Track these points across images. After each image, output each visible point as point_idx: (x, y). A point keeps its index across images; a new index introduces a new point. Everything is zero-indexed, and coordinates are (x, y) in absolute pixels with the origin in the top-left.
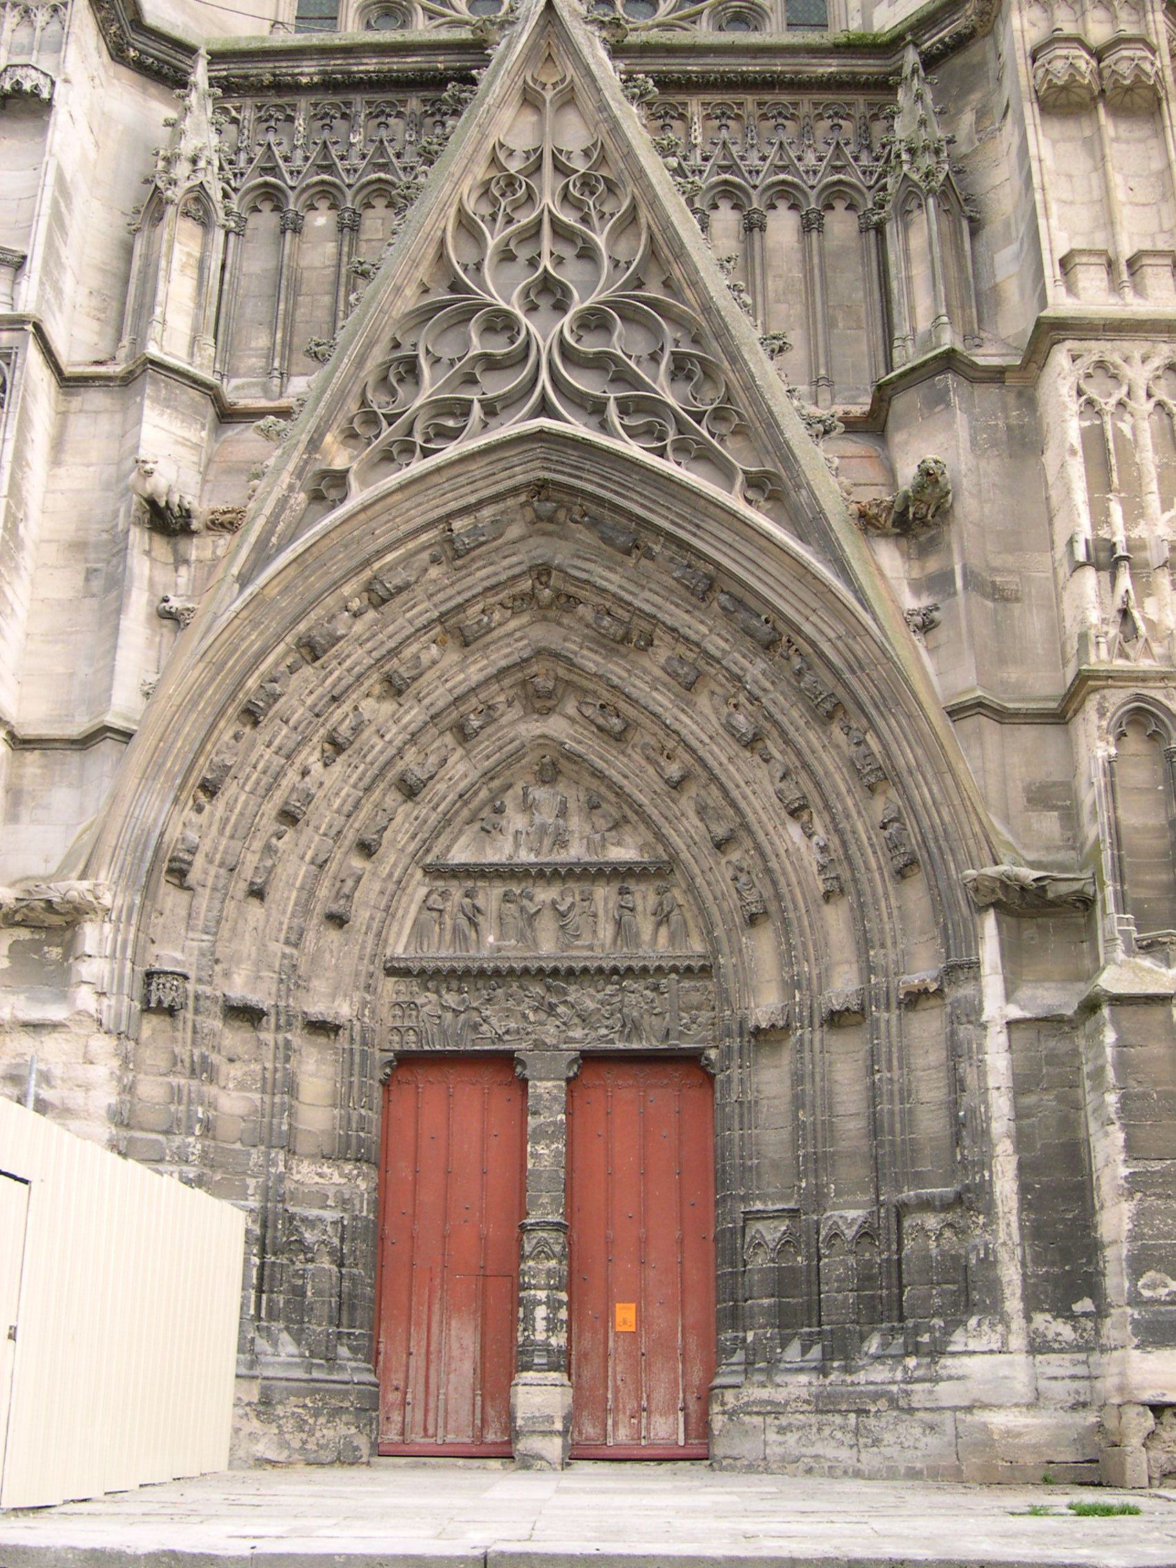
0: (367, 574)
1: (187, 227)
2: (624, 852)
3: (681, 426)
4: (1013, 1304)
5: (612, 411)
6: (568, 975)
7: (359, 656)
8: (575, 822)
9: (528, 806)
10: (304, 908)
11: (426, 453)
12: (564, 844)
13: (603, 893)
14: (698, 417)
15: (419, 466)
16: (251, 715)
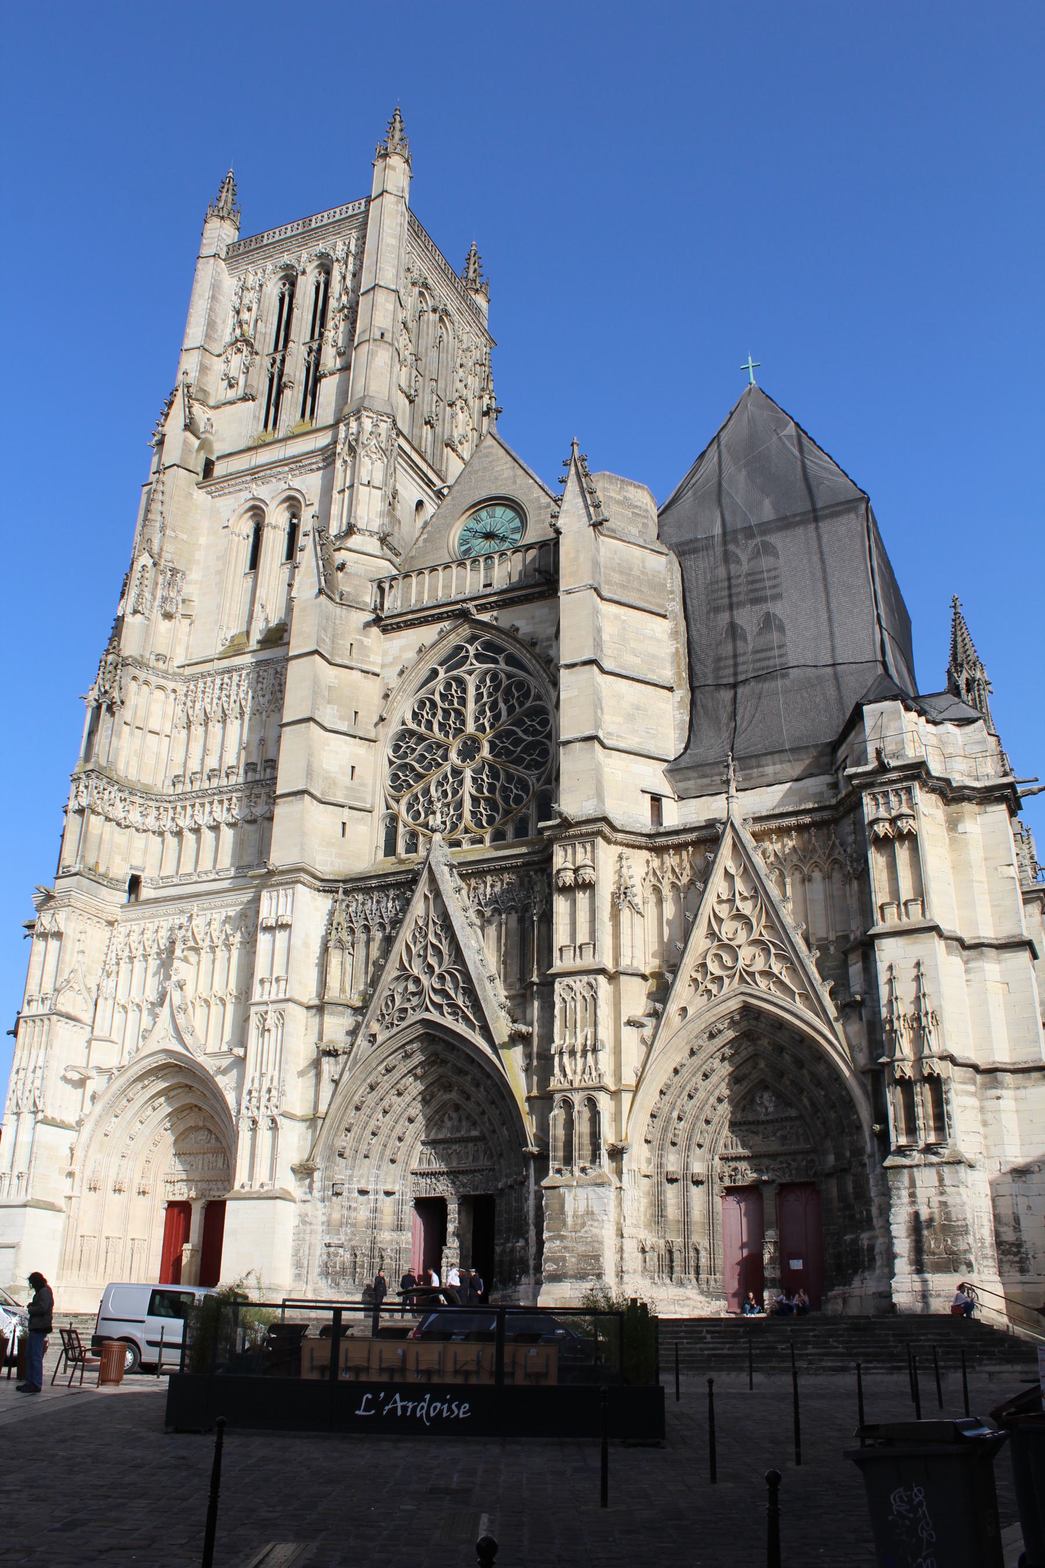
0: (385, 1063)
1: (338, 952)
2: (475, 1133)
3: (463, 1012)
4: (531, 1271)
5: (445, 1008)
6: (459, 1172)
7: (387, 1086)
8: (464, 1123)
9: (450, 1119)
10: (381, 1158)
11: (397, 1025)
12: (459, 1131)
13: (470, 1145)
14: (467, 1007)
15: (395, 1030)
16: (358, 1108)
